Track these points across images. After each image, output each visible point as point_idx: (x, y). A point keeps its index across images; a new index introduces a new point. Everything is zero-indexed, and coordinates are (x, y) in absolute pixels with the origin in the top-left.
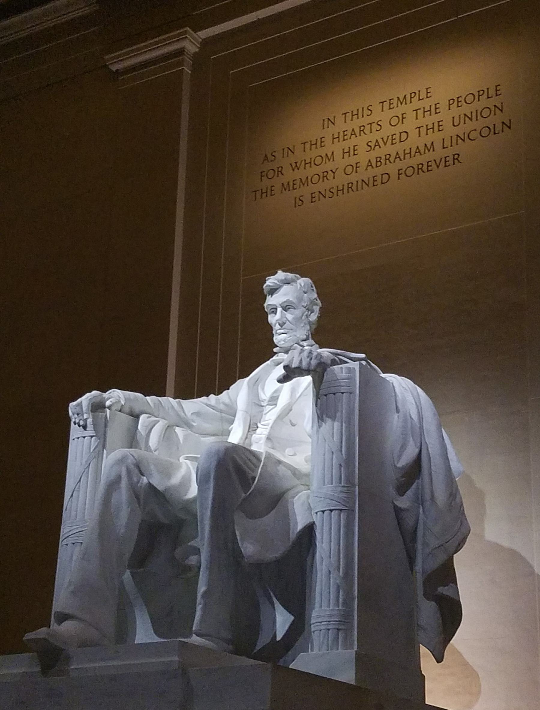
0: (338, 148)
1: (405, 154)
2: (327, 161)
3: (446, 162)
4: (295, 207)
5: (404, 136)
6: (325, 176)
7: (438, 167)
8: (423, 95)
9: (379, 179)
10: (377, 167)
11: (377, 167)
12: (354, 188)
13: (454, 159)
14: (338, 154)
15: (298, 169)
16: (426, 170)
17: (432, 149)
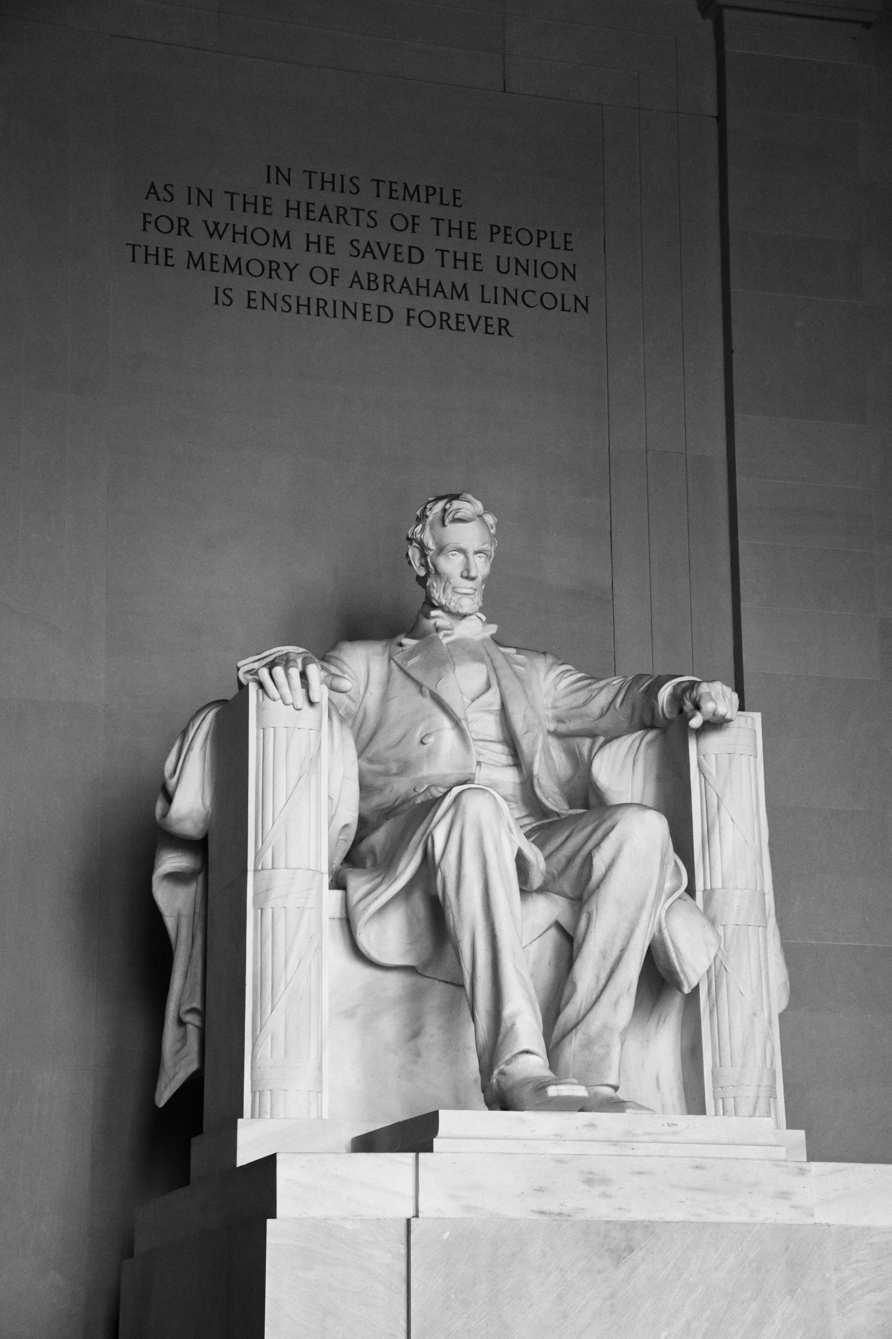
0: (299, 229)
1: (418, 287)
2: (277, 241)
3: (487, 325)
4: (217, 303)
5: (416, 256)
6: (272, 269)
7: (474, 329)
8: (448, 197)
9: (374, 310)
10: (369, 288)
11: (369, 288)
12: (329, 309)
13: (500, 327)
14: (299, 241)
15: (221, 237)
16: (454, 327)
17: (463, 295)
